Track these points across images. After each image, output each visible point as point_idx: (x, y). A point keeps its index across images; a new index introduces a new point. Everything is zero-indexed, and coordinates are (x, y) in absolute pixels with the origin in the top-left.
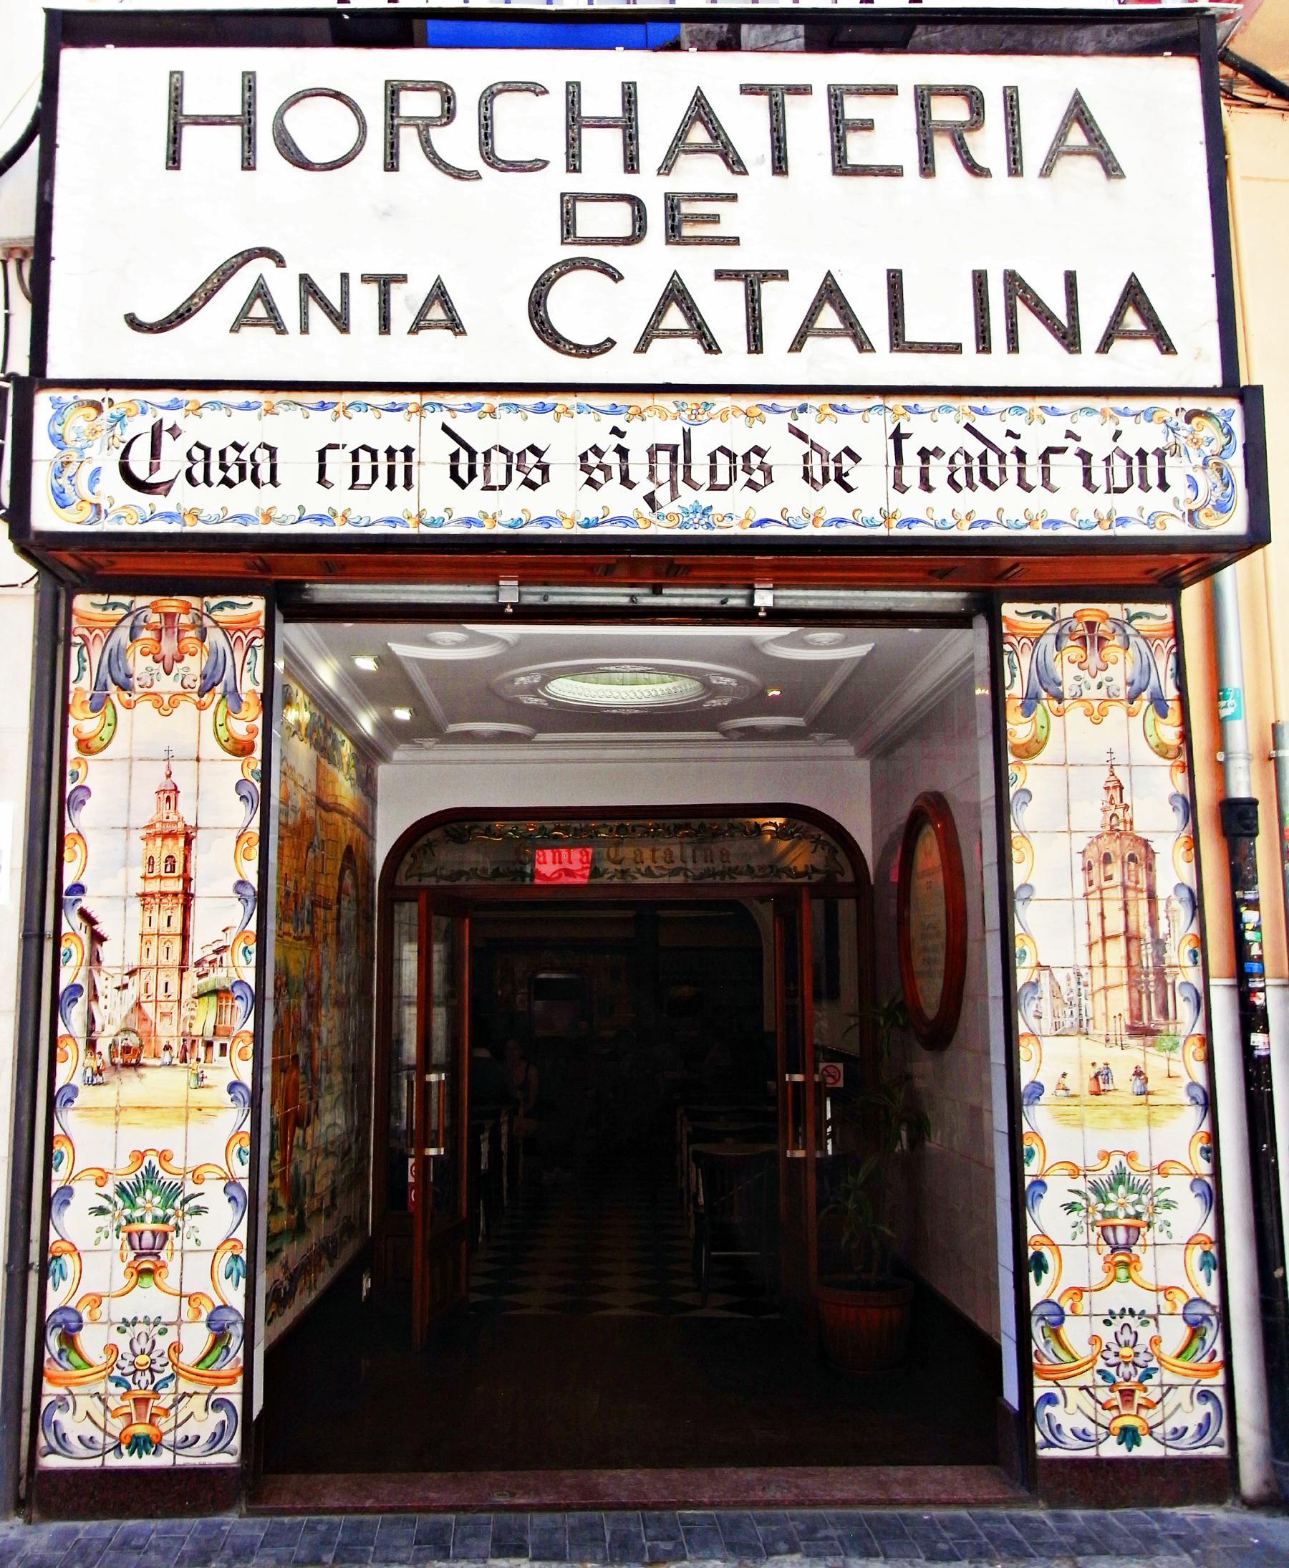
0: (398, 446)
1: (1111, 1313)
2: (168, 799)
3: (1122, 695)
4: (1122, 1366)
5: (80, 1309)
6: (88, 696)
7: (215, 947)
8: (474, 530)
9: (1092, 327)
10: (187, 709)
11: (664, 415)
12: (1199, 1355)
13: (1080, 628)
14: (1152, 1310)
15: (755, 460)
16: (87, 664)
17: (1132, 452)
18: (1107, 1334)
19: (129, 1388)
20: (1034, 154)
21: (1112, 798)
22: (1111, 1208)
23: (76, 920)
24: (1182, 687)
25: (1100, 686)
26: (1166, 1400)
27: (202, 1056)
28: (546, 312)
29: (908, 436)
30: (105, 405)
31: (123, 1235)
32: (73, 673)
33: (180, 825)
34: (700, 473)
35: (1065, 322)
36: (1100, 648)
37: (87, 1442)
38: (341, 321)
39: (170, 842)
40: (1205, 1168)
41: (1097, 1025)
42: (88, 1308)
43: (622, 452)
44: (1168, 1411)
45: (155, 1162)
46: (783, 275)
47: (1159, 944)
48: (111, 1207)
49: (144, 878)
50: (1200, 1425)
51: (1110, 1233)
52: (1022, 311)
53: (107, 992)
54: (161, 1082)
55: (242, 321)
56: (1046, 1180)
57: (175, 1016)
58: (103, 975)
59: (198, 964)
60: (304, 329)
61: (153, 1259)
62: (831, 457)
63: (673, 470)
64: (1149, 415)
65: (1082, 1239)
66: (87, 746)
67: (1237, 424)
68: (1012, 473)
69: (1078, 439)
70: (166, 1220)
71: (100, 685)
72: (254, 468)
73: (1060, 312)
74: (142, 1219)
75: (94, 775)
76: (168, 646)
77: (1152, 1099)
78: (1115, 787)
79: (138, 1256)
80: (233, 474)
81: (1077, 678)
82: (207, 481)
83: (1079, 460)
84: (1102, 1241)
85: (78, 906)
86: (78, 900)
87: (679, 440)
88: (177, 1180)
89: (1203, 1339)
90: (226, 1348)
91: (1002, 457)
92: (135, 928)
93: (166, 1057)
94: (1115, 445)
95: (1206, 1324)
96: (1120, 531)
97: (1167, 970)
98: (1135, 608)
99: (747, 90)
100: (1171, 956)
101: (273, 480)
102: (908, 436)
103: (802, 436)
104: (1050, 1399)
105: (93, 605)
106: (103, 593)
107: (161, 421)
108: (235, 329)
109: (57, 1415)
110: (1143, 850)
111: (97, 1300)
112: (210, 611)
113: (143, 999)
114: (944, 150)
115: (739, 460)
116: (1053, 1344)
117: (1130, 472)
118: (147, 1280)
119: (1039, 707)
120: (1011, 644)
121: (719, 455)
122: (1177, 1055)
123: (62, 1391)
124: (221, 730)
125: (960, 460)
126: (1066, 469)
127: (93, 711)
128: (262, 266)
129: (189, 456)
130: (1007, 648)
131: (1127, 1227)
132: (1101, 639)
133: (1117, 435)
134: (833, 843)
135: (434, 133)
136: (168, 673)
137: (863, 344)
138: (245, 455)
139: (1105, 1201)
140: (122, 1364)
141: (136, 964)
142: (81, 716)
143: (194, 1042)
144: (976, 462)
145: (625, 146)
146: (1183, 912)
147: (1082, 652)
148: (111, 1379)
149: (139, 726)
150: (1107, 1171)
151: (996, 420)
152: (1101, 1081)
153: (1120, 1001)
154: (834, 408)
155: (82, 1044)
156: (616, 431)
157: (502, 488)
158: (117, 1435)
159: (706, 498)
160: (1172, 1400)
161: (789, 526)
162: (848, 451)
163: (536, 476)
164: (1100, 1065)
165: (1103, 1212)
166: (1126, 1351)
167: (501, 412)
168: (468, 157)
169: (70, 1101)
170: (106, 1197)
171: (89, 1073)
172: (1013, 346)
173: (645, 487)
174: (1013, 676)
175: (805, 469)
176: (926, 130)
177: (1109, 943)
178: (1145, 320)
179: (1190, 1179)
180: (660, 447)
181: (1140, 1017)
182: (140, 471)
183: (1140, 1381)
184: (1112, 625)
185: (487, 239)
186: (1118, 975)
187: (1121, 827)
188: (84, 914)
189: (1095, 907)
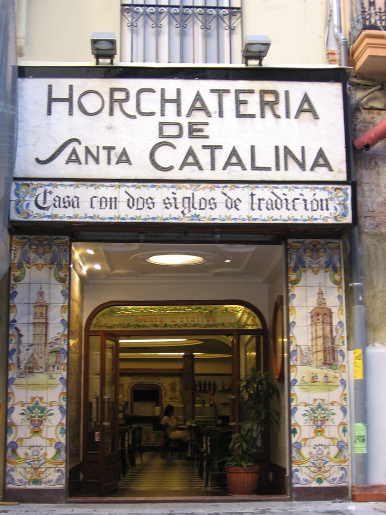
3: (324, 266)
8: (134, 221)
9: (309, 163)
11: (187, 188)
13: (311, 246)
14: (327, 445)
18: (314, 451)
19: (31, 465)
20: (294, 110)
22: (316, 415)
23: (14, 330)
25: (317, 263)
29: (255, 195)
30: (30, 185)
37: (20, 481)
38: (97, 160)
39: (41, 308)
44: (331, 473)
46: (220, 147)
47: (333, 339)
48: (25, 413)
49: (34, 318)
53: (23, 351)
54: (40, 378)
55: (69, 161)
56: (298, 407)
59: (50, 343)
60: (86, 163)
62: (234, 200)
63: (189, 204)
64: (324, 189)
65: (307, 424)
67: (349, 191)
68: (284, 205)
69: (303, 196)
70: (41, 417)
72: (72, 203)
76: (41, 250)
80: (67, 204)
81: (310, 261)
82: (60, 207)
83: (303, 202)
87: (191, 196)
88: (45, 406)
91: (281, 201)
92: (31, 333)
96: (315, 222)
98: (328, 241)
99: (213, 91)
101: (78, 207)
102: (255, 195)
103: (225, 194)
104: (297, 470)
108: (67, 163)
109: (11, 473)
111: (21, 439)
114: (268, 113)
115: (208, 201)
116: (298, 455)
117: (318, 205)
118: (36, 435)
123: (12, 466)
125: (269, 201)
126: (300, 205)
129: (55, 200)
132: (318, 250)
133: (315, 194)
135: (123, 104)
137: (244, 168)
140: (30, 458)
144: (274, 202)
147: (311, 253)
151: (280, 190)
152: (314, 379)
153: (321, 356)
155: (16, 365)
156: (173, 193)
157: (141, 209)
159: (198, 212)
160: (332, 470)
162: (238, 199)
163: (151, 206)
166: (320, 456)
167: (141, 187)
169: (13, 382)
170: (24, 410)
171: (18, 374)
172: (286, 169)
173: (181, 209)
174: (291, 260)
176: (263, 104)
179: (340, 407)
181: (326, 360)
182: (41, 204)
183: (323, 465)
186: (320, 348)
188: (16, 329)
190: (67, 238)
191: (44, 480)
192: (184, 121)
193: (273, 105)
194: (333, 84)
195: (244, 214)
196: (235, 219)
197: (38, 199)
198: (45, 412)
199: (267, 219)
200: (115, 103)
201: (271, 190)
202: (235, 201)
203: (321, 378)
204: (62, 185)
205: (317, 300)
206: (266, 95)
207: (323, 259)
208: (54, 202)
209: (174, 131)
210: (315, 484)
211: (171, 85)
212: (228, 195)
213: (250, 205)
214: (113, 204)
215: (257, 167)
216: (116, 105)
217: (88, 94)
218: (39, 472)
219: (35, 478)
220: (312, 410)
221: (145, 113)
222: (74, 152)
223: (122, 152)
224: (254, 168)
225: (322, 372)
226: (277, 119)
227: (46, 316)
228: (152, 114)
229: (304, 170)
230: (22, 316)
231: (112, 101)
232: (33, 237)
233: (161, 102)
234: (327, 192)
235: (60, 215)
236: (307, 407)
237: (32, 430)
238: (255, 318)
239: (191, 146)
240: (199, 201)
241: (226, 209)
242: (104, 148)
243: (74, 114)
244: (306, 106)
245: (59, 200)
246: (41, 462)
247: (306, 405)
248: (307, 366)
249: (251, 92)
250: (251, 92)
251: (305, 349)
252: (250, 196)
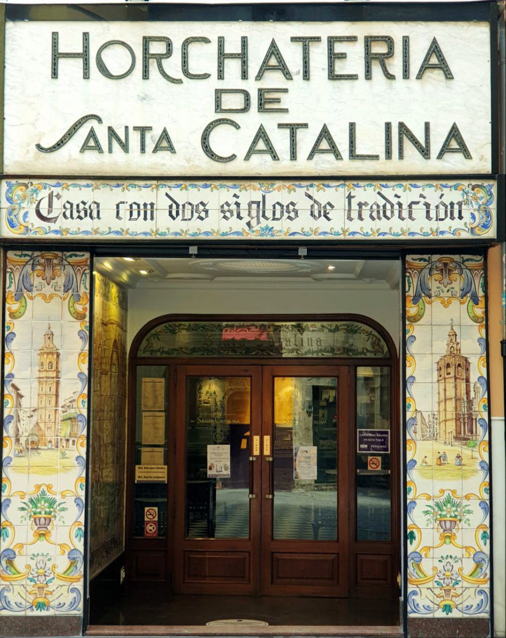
0: (148, 203)
1: (442, 557)
2: (49, 338)
4: (446, 580)
5: (14, 550)
6: (14, 294)
7: (70, 400)
9: (436, 147)
10: (56, 300)
11: (254, 189)
12: (479, 575)
13: (440, 265)
14: (460, 556)
15: (291, 207)
16: (13, 280)
17: (448, 203)
18: (440, 566)
19: (36, 582)
20: (415, 68)
21: (452, 339)
22: (444, 513)
25: (448, 291)
26: (464, 594)
27: (65, 445)
28: (208, 142)
29: (354, 197)
30: (29, 185)
31: (32, 519)
32: (7, 285)
33: (54, 349)
35: (424, 145)
36: (449, 275)
38: (125, 147)
39: (50, 356)
40: (486, 497)
41: (441, 436)
42: (18, 549)
43: (238, 204)
44: (465, 598)
45: (45, 489)
46: (305, 126)
47: (470, 402)
48: (27, 508)
49: (39, 371)
50: (478, 605)
51: (443, 523)
52: (406, 141)
53: (24, 418)
54: (46, 456)
55: (85, 147)
56: (417, 501)
57: (53, 429)
58: (22, 412)
59: (62, 407)
60: (110, 151)
61: (45, 529)
63: (258, 212)
64: (456, 188)
65: (431, 526)
66: (14, 316)
68: (396, 213)
69: (424, 198)
70: (50, 513)
72: (90, 212)
73: (422, 141)
74: (40, 513)
76: (49, 273)
77: (464, 468)
78: (453, 335)
79: (39, 528)
80: (82, 214)
82: (72, 217)
84: (440, 527)
85: (11, 383)
86: (11, 380)
87: (261, 199)
89: (482, 569)
90: (76, 566)
91: (392, 206)
93: (50, 446)
94: (440, 200)
95: (483, 562)
96: (441, 237)
97: (473, 413)
98: (466, 257)
99: (294, 39)
100: (476, 407)
101: (98, 217)
102: (354, 197)
103: (310, 197)
104: (414, 593)
105: (15, 255)
106: (20, 250)
107: (52, 192)
109: (6, 594)
110: (465, 362)
111: (21, 546)
112: (66, 258)
113: (39, 421)
114: (376, 69)
115: (285, 208)
116: (417, 570)
118: (42, 538)
119: (421, 300)
120: (409, 273)
121: (277, 205)
122: (476, 449)
123: (8, 583)
124: (71, 309)
125: (375, 207)
126: (419, 211)
127: (16, 300)
130: (408, 274)
131: (451, 521)
132: (450, 270)
133: (442, 195)
134: (379, 336)
136: (48, 284)
137: (338, 156)
138: (87, 206)
139: (441, 510)
140: (33, 573)
141: (36, 406)
142: (11, 303)
143: (61, 439)
144: (381, 208)
145: (242, 66)
146: (482, 389)
147: (440, 276)
148: (28, 579)
150: (443, 497)
151: (390, 191)
152: (441, 460)
153: (451, 426)
154: (324, 185)
155: (13, 440)
156: (235, 196)
157: (190, 220)
158: (31, 601)
159: (271, 223)
160: (466, 594)
161: (305, 235)
162: (329, 204)
163: (203, 214)
164: (442, 453)
165: (440, 515)
166: (448, 573)
167: (190, 188)
169: (9, 463)
170: (25, 503)
171: (17, 452)
172: (401, 156)
173: (246, 219)
174: (410, 286)
175: (312, 212)
176: (369, 58)
177: (448, 402)
178: (459, 144)
179: (479, 501)
180: (253, 202)
181: (460, 434)
182: (44, 213)
183: (453, 586)
184: (455, 264)
185: (182, 109)
186: (451, 415)
187: (455, 352)
188: (13, 386)
189: (442, 386)
190: (87, 255)
191: (52, 604)
192: (252, 86)
193: (383, 59)
194: (477, 24)
195: (336, 227)
196: (325, 233)
197: (41, 206)
198: (55, 506)
199: (370, 232)
200: (151, 60)
201: (378, 190)
202: (325, 207)
203: (451, 459)
204: (75, 185)
205: (448, 345)
206: (373, 44)
207: (458, 285)
208: (64, 210)
209: (236, 101)
210: (440, 614)
211: (232, 32)
212: (315, 197)
213: (346, 212)
214: (149, 213)
215: (358, 156)
217: (111, 46)
218: (45, 592)
219: (41, 600)
220: (437, 505)
221: (195, 76)
222: (92, 134)
223: (162, 135)
225: (453, 450)
226: (389, 81)
227: (57, 368)
228: (206, 76)
229: (429, 158)
230: (21, 366)
232: (36, 253)
233: (219, 58)
234: (462, 192)
236: (431, 500)
237: (35, 532)
238: (379, 339)
239: (261, 125)
240: (272, 208)
241: (312, 218)
242: (135, 128)
243: (91, 76)
244: (434, 60)
245: (72, 207)
246: (48, 578)
247: (429, 498)
248: (431, 442)
249: (352, 39)
250: (352, 39)
251: (429, 416)
252: (347, 200)
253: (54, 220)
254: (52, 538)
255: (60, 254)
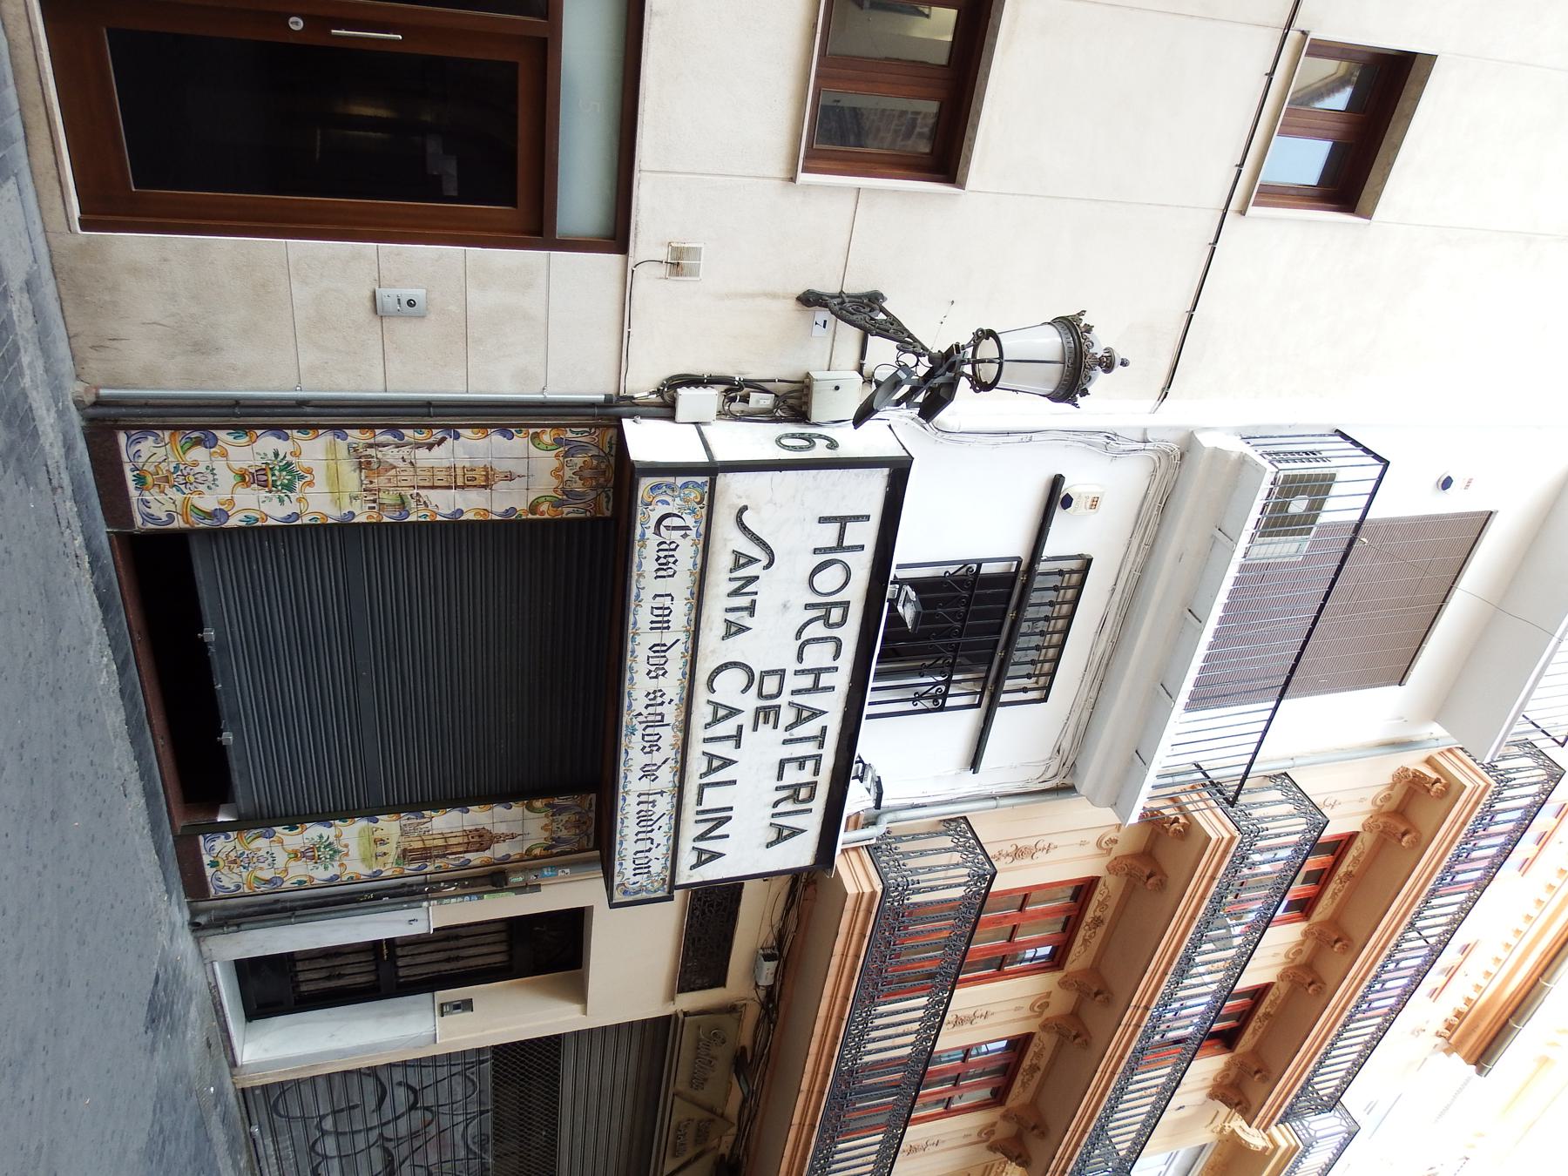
9: (703, 845)
10: (555, 482)
23: (439, 436)
24: (558, 854)
34: (649, 731)
37: (137, 454)
38: (735, 593)
47: (444, 856)
54: (351, 479)
55: (738, 555)
64: (665, 868)
67: (660, 894)
71: (568, 442)
72: (665, 567)
75: (520, 443)
76: (587, 473)
99: (824, 729)
111: (225, 455)
126: (641, 846)
128: (765, 562)
149: (545, 461)
152: (383, 842)
159: (639, 734)
168: (807, 634)
173: (645, 712)
176: (796, 788)
182: (666, 522)
185: (769, 642)
186: (429, 844)
188: (443, 440)
193: (794, 798)
204: (696, 552)
210: (206, 859)
216: (821, 612)
219: (149, 479)
222: (752, 560)
224: (702, 788)
225: (392, 850)
228: (800, 658)
231: (829, 607)
232: (612, 460)
235: (645, 552)
242: (754, 602)
253: (657, 532)
254: (239, 489)
255: (611, 484)
